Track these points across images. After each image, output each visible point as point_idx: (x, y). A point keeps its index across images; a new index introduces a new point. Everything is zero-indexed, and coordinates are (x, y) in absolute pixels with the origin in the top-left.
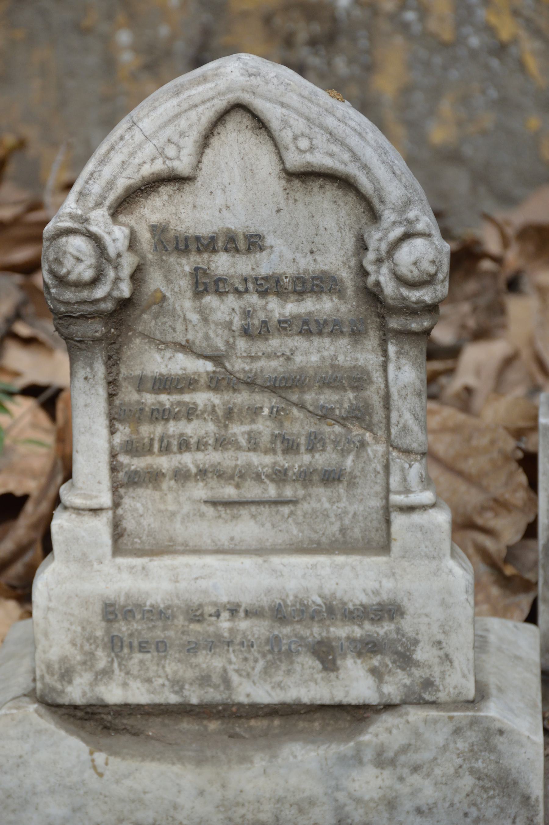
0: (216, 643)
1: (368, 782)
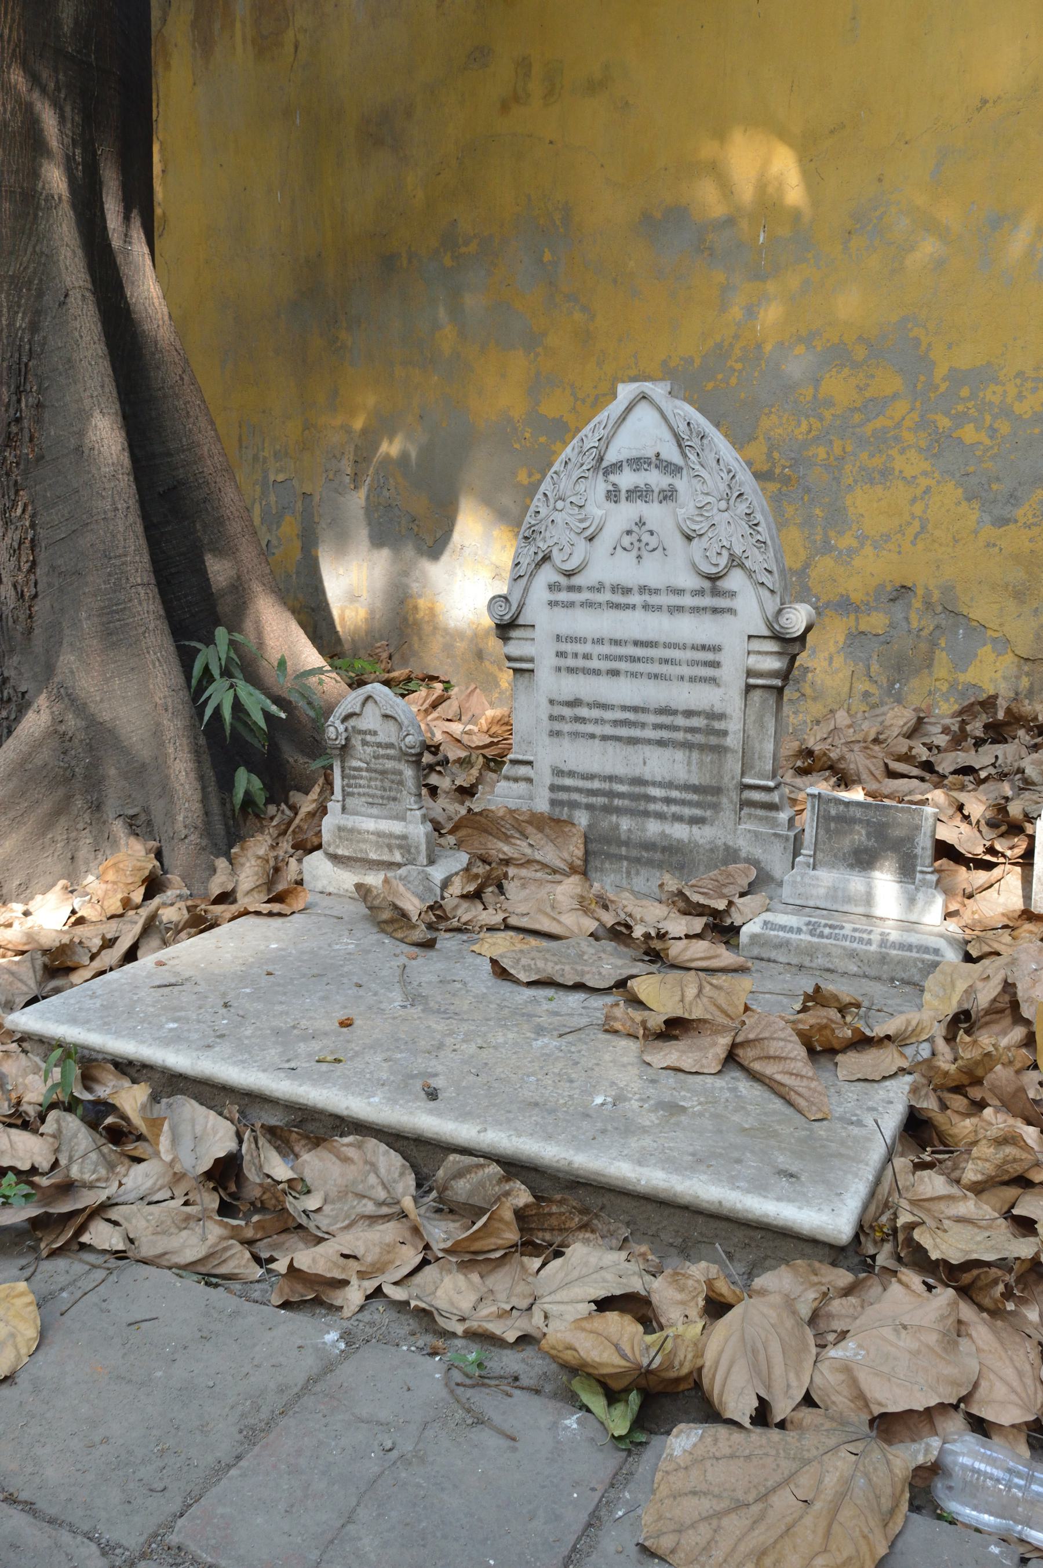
0: (365, 841)
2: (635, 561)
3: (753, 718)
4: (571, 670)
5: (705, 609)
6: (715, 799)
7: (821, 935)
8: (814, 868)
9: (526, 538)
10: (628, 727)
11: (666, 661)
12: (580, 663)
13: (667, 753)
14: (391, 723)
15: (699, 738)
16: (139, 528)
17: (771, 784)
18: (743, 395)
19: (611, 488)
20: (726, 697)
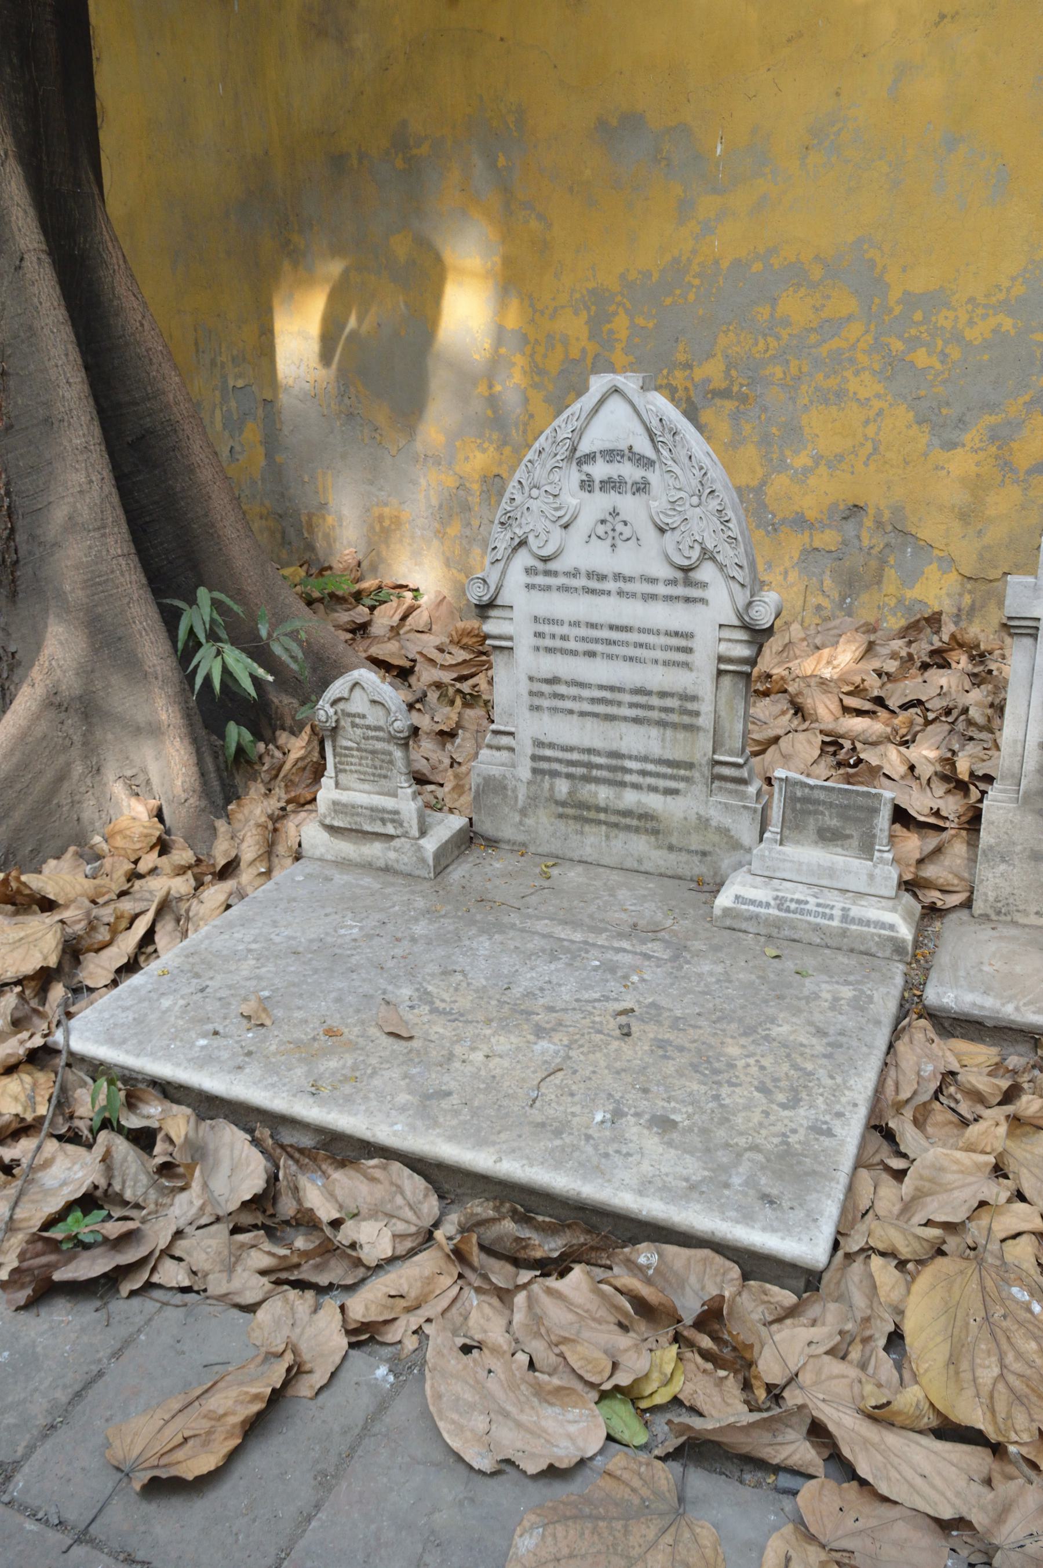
0: (358, 814)
1: (392, 855)
2: (610, 549)
3: (723, 700)
4: (549, 650)
5: (677, 598)
6: (687, 773)
7: (788, 910)
8: (781, 844)
9: (502, 524)
10: (605, 704)
11: (641, 645)
12: (558, 643)
13: (642, 730)
14: (379, 708)
15: (674, 718)
16: (115, 499)
17: (741, 761)
18: (701, 312)
19: (584, 478)
20: (699, 679)
